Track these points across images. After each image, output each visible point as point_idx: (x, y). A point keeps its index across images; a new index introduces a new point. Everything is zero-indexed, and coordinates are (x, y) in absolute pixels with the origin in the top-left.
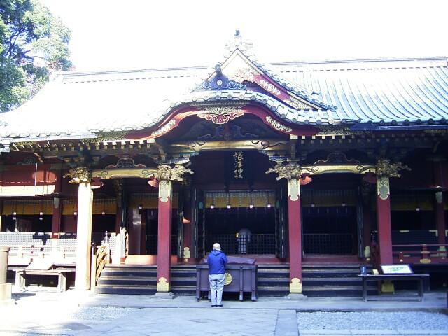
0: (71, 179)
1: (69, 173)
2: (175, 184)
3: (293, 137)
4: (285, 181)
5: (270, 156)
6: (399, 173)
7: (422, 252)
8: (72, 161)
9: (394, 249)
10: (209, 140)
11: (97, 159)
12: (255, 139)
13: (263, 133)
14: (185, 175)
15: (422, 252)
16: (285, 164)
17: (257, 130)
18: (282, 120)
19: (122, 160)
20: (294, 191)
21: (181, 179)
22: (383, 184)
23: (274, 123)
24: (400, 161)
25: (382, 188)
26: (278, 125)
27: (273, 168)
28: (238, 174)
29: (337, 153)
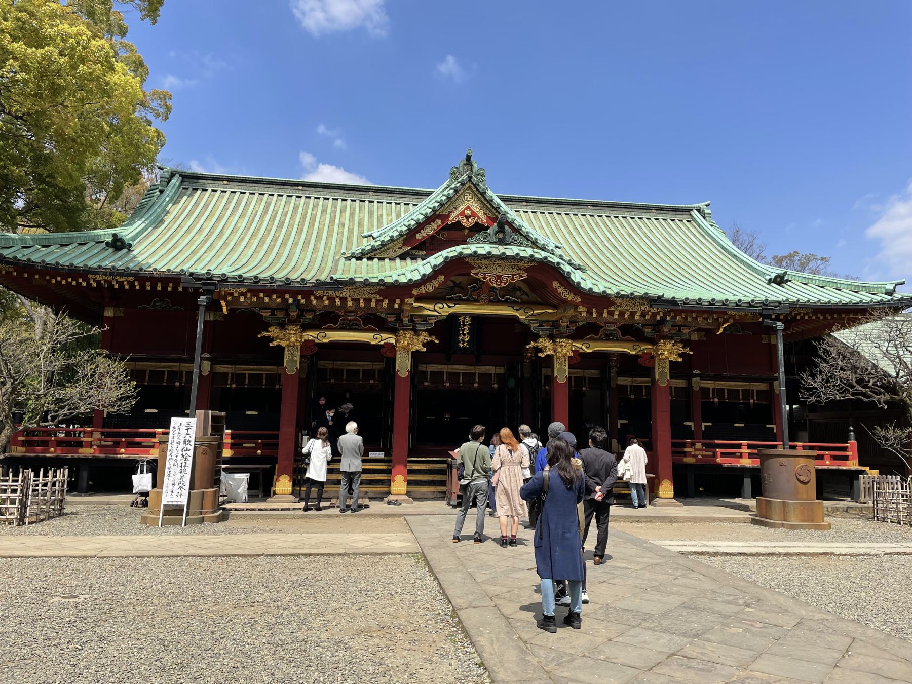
0: (272, 340)
1: (268, 332)
2: (416, 355)
4: (549, 357)
5: (534, 326)
6: (680, 355)
7: (686, 450)
8: (273, 314)
9: (673, 445)
10: (459, 301)
11: (309, 316)
13: (525, 297)
15: (686, 450)
16: (552, 338)
17: (518, 294)
18: (575, 288)
19: (347, 319)
20: (561, 372)
21: (425, 349)
22: (663, 367)
23: (561, 290)
24: (681, 342)
25: (662, 373)
26: (565, 293)
27: (536, 342)
28: (464, 341)
29: (612, 328)
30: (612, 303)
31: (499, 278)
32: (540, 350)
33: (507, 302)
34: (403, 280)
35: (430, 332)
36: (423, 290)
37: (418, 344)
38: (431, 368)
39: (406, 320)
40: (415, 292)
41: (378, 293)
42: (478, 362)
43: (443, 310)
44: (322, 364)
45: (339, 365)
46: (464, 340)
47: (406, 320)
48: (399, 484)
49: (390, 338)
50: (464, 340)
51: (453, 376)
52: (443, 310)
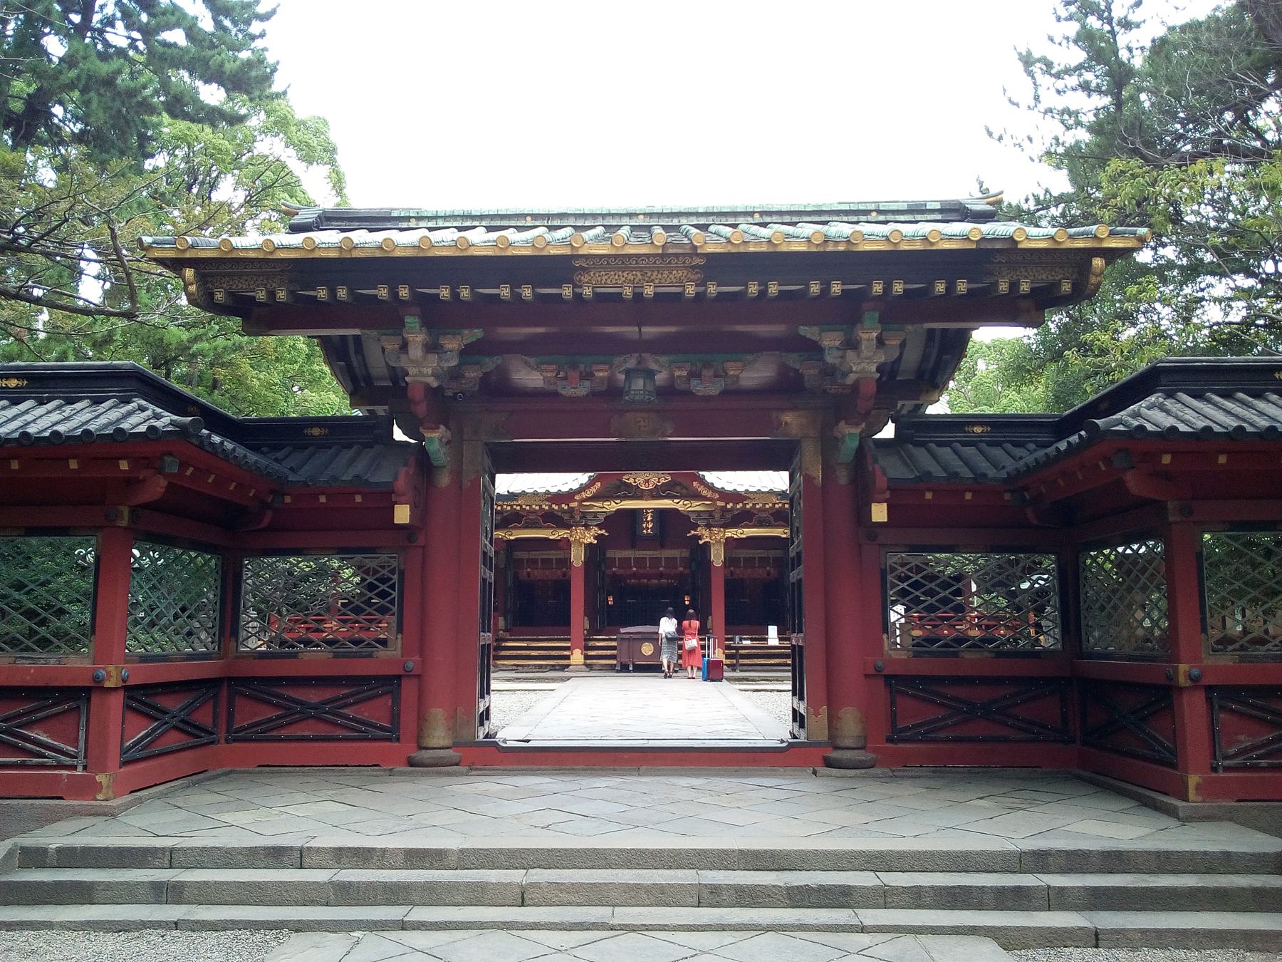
2: (589, 547)
3: (720, 504)
4: (707, 544)
5: (692, 516)
12: (676, 497)
14: (597, 537)
16: (709, 526)
17: (678, 488)
18: (711, 487)
20: (717, 557)
29: (763, 515)
31: (647, 481)
32: (700, 538)
33: (667, 497)
34: (565, 489)
35: (600, 527)
36: (584, 495)
37: (589, 538)
39: (578, 518)
40: (577, 497)
41: (547, 500)
42: (662, 546)
43: (612, 506)
44: (519, 555)
45: (534, 555)
46: (648, 526)
47: (578, 518)
48: (577, 657)
49: (562, 534)
50: (648, 526)
52: (612, 506)
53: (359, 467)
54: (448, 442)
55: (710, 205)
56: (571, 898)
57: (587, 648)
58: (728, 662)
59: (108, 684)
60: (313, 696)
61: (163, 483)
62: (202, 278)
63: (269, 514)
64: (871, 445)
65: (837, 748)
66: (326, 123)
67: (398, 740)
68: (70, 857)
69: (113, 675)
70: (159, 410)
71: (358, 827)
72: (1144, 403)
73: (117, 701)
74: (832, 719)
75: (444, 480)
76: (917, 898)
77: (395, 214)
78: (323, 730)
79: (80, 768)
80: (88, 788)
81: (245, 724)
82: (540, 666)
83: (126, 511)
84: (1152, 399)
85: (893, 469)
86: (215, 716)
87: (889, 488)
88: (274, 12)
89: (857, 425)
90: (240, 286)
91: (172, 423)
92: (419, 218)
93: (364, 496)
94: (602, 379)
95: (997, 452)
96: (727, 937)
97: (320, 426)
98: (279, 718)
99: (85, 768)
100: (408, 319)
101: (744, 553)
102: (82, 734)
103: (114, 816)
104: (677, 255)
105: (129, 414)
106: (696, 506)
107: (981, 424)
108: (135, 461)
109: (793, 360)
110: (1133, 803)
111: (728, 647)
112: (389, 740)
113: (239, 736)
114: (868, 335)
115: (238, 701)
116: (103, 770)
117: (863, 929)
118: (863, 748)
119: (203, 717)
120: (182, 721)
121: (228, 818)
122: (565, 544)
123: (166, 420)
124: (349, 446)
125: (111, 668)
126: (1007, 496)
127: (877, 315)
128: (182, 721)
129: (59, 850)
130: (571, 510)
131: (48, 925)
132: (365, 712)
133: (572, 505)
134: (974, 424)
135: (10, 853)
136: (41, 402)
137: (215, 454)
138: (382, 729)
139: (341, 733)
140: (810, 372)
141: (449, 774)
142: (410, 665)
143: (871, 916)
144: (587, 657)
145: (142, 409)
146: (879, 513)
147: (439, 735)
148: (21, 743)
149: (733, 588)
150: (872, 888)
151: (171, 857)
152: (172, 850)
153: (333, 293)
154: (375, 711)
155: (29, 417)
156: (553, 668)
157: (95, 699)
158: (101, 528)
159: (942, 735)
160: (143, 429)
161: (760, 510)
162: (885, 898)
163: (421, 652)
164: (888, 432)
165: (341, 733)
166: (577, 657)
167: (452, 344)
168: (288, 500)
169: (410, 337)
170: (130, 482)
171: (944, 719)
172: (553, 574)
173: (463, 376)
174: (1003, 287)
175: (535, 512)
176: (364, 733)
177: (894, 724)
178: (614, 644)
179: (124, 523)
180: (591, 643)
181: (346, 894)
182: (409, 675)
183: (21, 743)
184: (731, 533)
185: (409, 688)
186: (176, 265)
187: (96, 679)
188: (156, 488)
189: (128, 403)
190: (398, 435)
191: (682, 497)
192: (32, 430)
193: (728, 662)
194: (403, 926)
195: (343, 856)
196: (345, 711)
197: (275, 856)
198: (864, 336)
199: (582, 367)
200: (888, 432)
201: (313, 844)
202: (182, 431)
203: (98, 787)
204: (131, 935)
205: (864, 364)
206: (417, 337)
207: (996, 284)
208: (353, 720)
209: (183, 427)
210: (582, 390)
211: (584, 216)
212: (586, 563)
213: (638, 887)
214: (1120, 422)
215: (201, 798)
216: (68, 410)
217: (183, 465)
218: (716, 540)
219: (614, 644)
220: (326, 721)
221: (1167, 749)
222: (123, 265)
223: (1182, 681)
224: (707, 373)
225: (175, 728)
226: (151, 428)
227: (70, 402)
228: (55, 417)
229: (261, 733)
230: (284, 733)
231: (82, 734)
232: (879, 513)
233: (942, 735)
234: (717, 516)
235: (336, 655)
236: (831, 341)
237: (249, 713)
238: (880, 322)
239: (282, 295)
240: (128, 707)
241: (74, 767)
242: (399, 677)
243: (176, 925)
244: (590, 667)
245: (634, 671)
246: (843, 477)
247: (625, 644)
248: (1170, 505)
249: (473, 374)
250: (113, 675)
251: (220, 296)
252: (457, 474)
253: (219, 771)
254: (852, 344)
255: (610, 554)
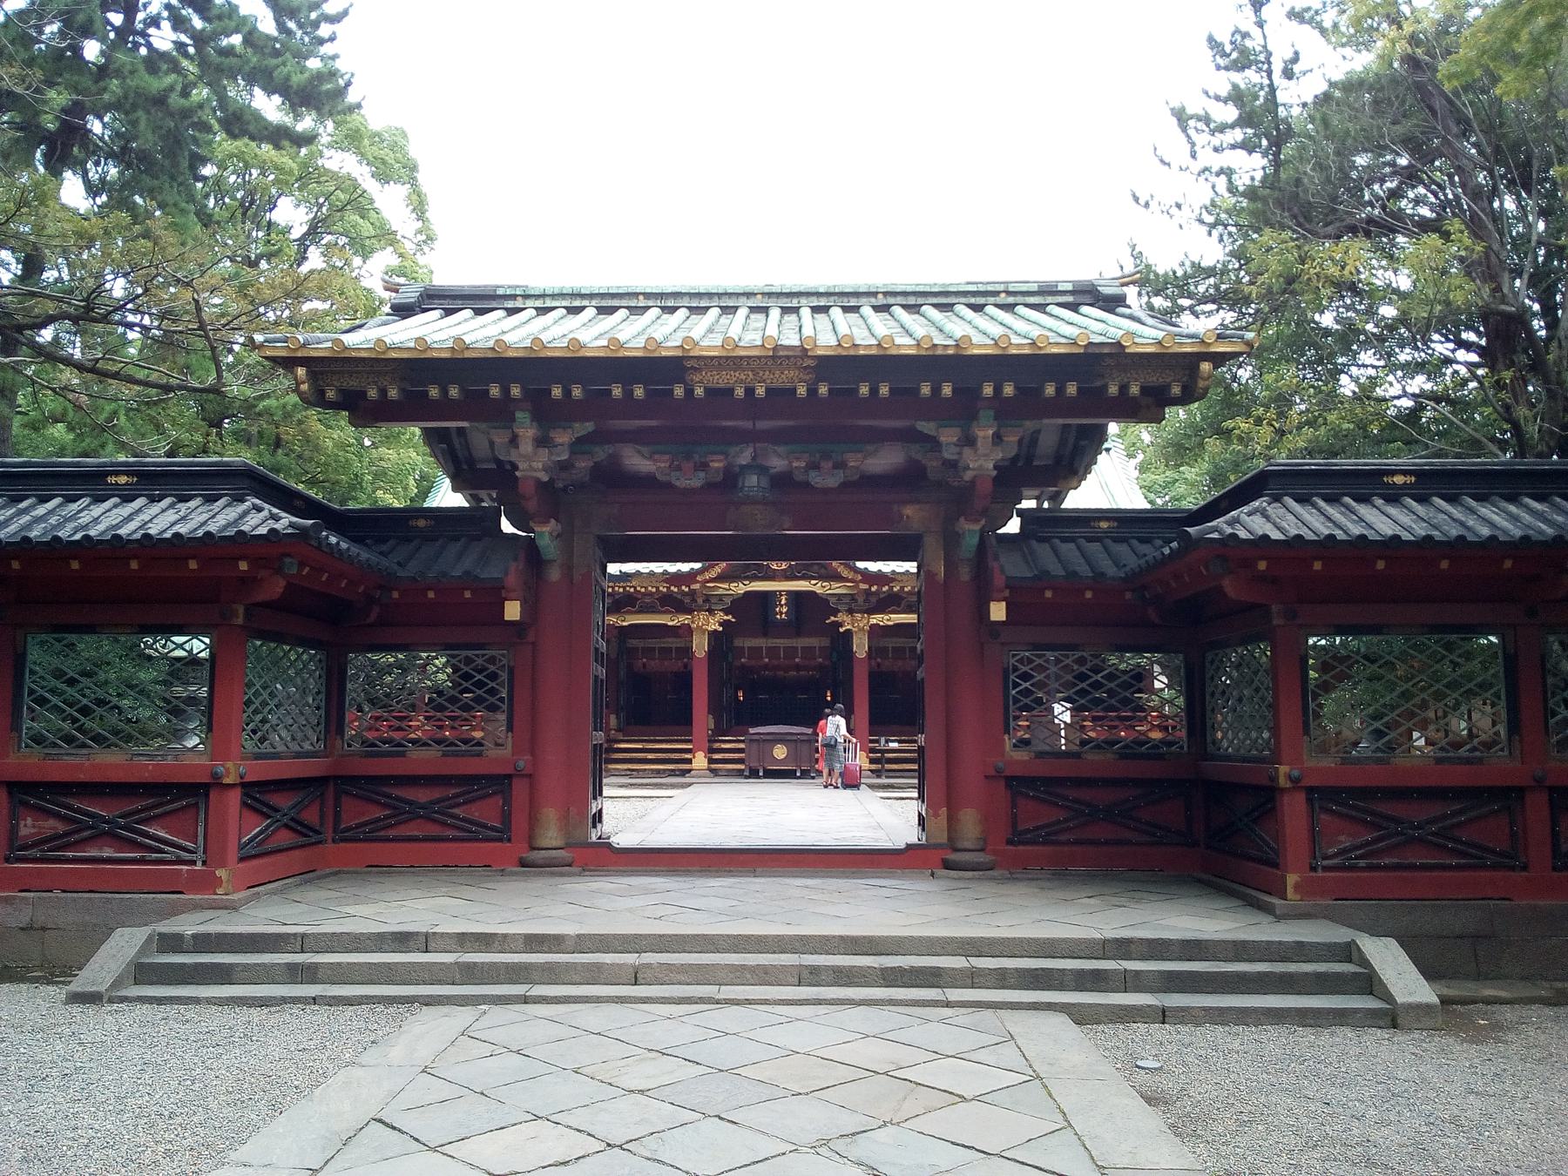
2: (713, 635)
3: (864, 586)
5: (832, 600)
16: (851, 612)
30: (893, 580)
35: (726, 612)
36: (707, 576)
37: (713, 625)
38: (749, 643)
39: (700, 601)
40: (699, 578)
41: (666, 581)
42: (798, 634)
43: (740, 588)
44: (633, 643)
46: (782, 611)
47: (700, 601)
48: (700, 761)
49: (683, 619)
50: (782, 611)
51: (773, 651)
52: (740, 588)
53: (467, 563)
54: (558, 536)
55: (831, 283)
56: (682, 978)
57: (712, 751)
58: (874, 767)
59: (227, 781)
60: (422, 795)
61: (282, 583)
62: (313, 376)
63: (376, 610)
64: (994, 541)
65: (956, 850)
66: (404, 135)
67: (509, 840)
68: (204, 943)
69: (232, 772)
70: (275, 511)
71: (477, 917)
72: (1246, 509)
73: (235, 797)
74: (952, 820)
75: (554, 574)
76: (1002, 979)
77: (500, 292)
78: (435, 830)
79: (199, 863)
80: (207, 883)
81: (352, 823)
82: (658, 771)
83: (241, 610)
84: (1256, 504)
85: (1011, 566)
86: (322, 817)
87: (1007, 587)
88: (345, 13)
89: (977, 521)
90: (353, 384)
91: (291, 525)
92: (526, 297)
93: (474, 592)
94: (717, 469)
95: (1122, 549)
96: (822, 1009)
97: (426, 518)
98: (386, 817)
99: (204, 863)
100: (519, 415)
101: (891, 643)
102: (201, 830)
103: (235, 909)
104: (788, 357)
105: (245, 513)
106: (837, 588)
107: (1107, 519)
108: (255, 562)
109: (916, 452)
110: (1240, 903)
111: (872, 751)
112: (501, 840)
113: (345, 836)
114: (984, 433)
115: (344, 799)
116: (223, 865)
117: (948, 1004)
118: (982, 850)
119: (311, 816)
120: (292, 819)
121: (350, 910)
122: (687, 631)
123: (285, 521)
124: (456, 539)
125: (230, 764)
126: (1128, 595)
127: (992, 413)
128: (292, 819)
129: (194, 936)
130: (693, 593)
131: (196, 1001)
132: (476, 812)
133: (696, 586)
134: (1100, 519)
135: (150, 939)
136: (154, 500)
137: (319, 548)
138: (493, 829)
139: (451, 833)
140: (932, 464)
141: (562, 875)
142: (521, 764)
143: (955, 994)
144: (711, 761)
145: (260, 510)
146: (998, 612)
147: (551, 835)
148: (140, 839)
149: (879, 681)
150: (961, 970)
151: (302, 942)
152: (303, 936)
153: (444, 391)
154: (485, 811)
155: (145, 517)
156: (672, 773)
157: (213, 795)
158: (216, 626)
159: (1063, 838)
160: (263, 530)
161: (909, 593)
162: (972, 979)
163: (532, 755)
164: (1013, 526)
165: (451, 833)
166: (700, 761)
167: (563, 438)
168: (395, 595)
169: (521, 432)
170: (246, 581)
171: (1066, 820)
172: (674, 665)
173: (573, 466)
174: (1113, 390)
175: (651, 594)
176: (473, 833)
177: (1014, 825)
178: (742, 746)
179: (240, 621)
180: (716, 745)
181: (471, 974)
182: (520, 774)
183: (140, 839)
184: (876, 619)
185: (520, 788)
186: (289, 363)
187: (215, 776)
188: (275, 588)
189: (243, 501)
190: (507, 527)
191: (821, 578)
192: (153, 530)
193: (874, 767)
194: (525, 1000)
195: (465, 941)
196: (456, 811)
197: (402, 940)
198: (980, 434)
199: (696, 457)
200: (1013, 526)
201: (436, 930)
202: (303, 533)
203: (218, 882)
204: (273, 1009)
205: (982, 461)
206: (527, 431)
207: (1105, 387)
208: (464, 820)
209: (304, 531)
210: (697, 481)
211: (699, 295)
212: (710, 653)
213: (743, 967)
214: (1215, 529)
215: (316, 894)
216: (183, 507)
217: (302, 564)
218: (858, 627)
219: (742, 746)
220: (434, 821)
221: (1272, 849)
222: (207, 337)
223: (1283, 782)
224: (827, 465)
225: (286, 826)
226: (272, 531)
227: (184, 499)
228: (171, 516)
229: (369, 834)
230: (392, 833)
231: (201, 830)
232: (998, 612)
233: (1063, 838)
234: (861, 600)
235: (445, 755)
236: (949, 436)
237: (356, 812)
238: (996, 418)
239: (393, 393)
240: (244, 804)
241: (194, 863)
242: (509, 777)
243: (314, 1000)
244: (715, 772)
245: (765, 776)
246: (965, 574)
247: (755, 745)
248: (1274, 608)
249: (583, 464)
250: (232, 772)
251: (331, 394)
252: (568, 569)
253: (328, 871)
254: (969, 441)
255: (738, 642)
